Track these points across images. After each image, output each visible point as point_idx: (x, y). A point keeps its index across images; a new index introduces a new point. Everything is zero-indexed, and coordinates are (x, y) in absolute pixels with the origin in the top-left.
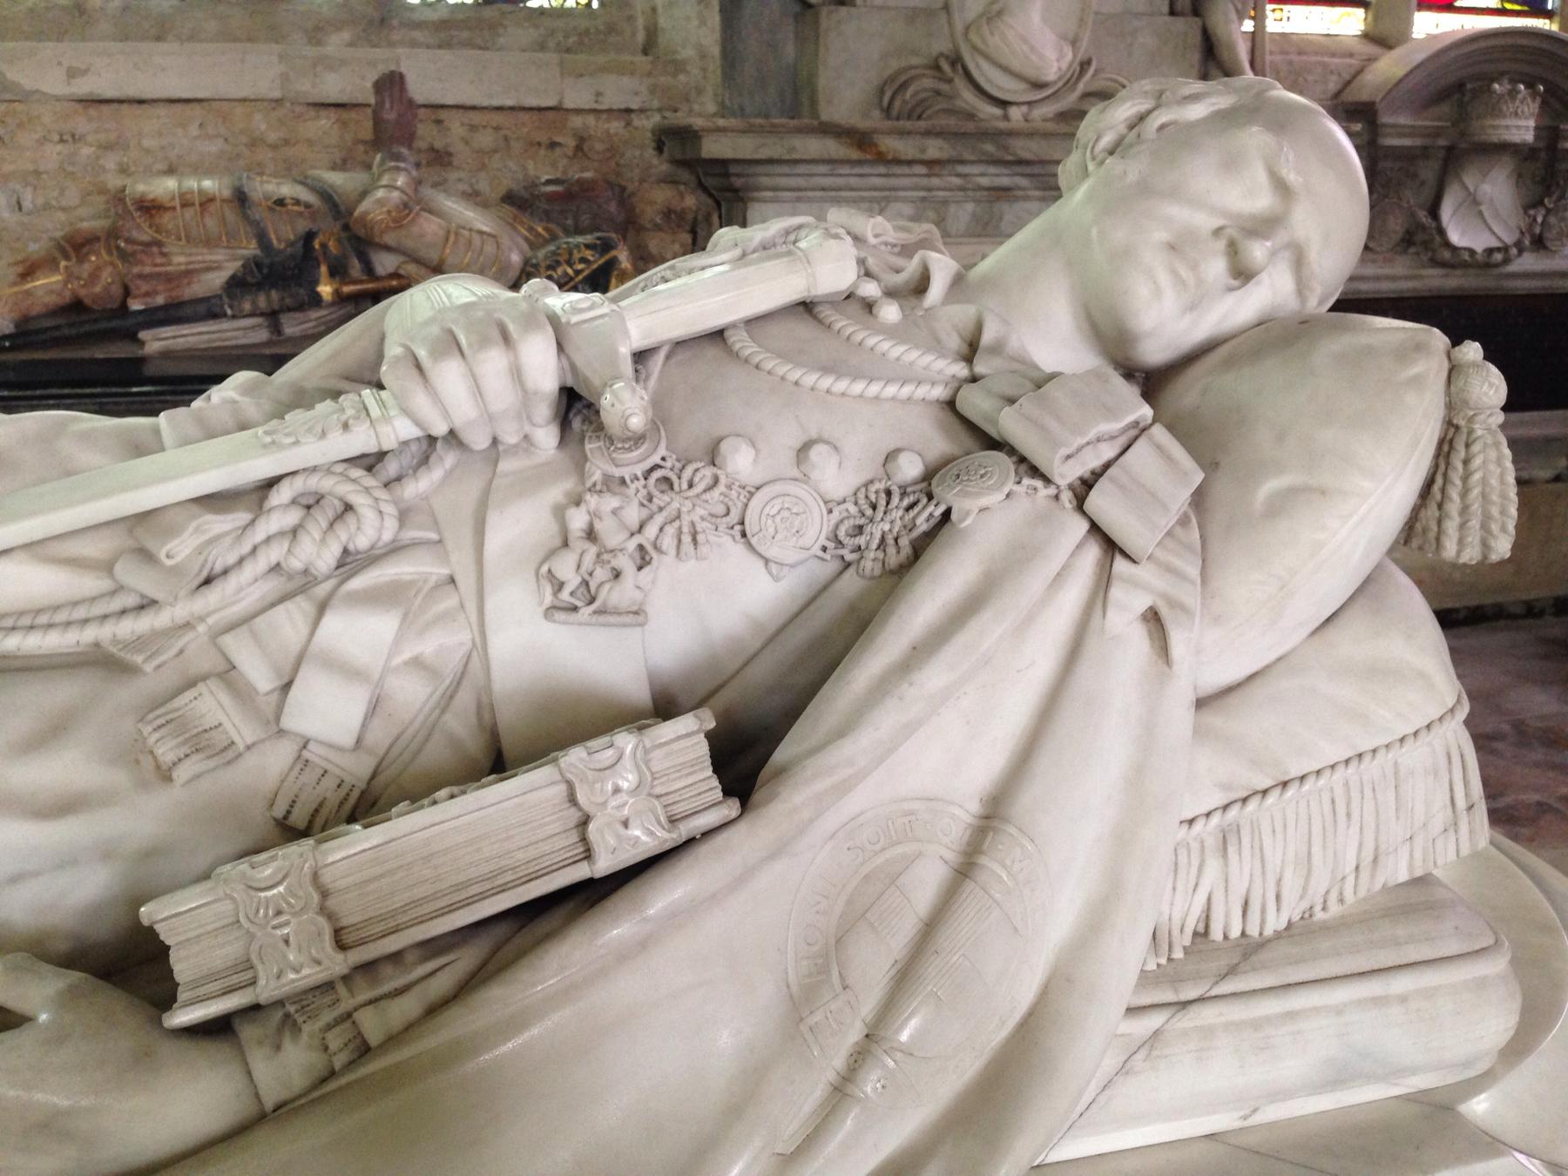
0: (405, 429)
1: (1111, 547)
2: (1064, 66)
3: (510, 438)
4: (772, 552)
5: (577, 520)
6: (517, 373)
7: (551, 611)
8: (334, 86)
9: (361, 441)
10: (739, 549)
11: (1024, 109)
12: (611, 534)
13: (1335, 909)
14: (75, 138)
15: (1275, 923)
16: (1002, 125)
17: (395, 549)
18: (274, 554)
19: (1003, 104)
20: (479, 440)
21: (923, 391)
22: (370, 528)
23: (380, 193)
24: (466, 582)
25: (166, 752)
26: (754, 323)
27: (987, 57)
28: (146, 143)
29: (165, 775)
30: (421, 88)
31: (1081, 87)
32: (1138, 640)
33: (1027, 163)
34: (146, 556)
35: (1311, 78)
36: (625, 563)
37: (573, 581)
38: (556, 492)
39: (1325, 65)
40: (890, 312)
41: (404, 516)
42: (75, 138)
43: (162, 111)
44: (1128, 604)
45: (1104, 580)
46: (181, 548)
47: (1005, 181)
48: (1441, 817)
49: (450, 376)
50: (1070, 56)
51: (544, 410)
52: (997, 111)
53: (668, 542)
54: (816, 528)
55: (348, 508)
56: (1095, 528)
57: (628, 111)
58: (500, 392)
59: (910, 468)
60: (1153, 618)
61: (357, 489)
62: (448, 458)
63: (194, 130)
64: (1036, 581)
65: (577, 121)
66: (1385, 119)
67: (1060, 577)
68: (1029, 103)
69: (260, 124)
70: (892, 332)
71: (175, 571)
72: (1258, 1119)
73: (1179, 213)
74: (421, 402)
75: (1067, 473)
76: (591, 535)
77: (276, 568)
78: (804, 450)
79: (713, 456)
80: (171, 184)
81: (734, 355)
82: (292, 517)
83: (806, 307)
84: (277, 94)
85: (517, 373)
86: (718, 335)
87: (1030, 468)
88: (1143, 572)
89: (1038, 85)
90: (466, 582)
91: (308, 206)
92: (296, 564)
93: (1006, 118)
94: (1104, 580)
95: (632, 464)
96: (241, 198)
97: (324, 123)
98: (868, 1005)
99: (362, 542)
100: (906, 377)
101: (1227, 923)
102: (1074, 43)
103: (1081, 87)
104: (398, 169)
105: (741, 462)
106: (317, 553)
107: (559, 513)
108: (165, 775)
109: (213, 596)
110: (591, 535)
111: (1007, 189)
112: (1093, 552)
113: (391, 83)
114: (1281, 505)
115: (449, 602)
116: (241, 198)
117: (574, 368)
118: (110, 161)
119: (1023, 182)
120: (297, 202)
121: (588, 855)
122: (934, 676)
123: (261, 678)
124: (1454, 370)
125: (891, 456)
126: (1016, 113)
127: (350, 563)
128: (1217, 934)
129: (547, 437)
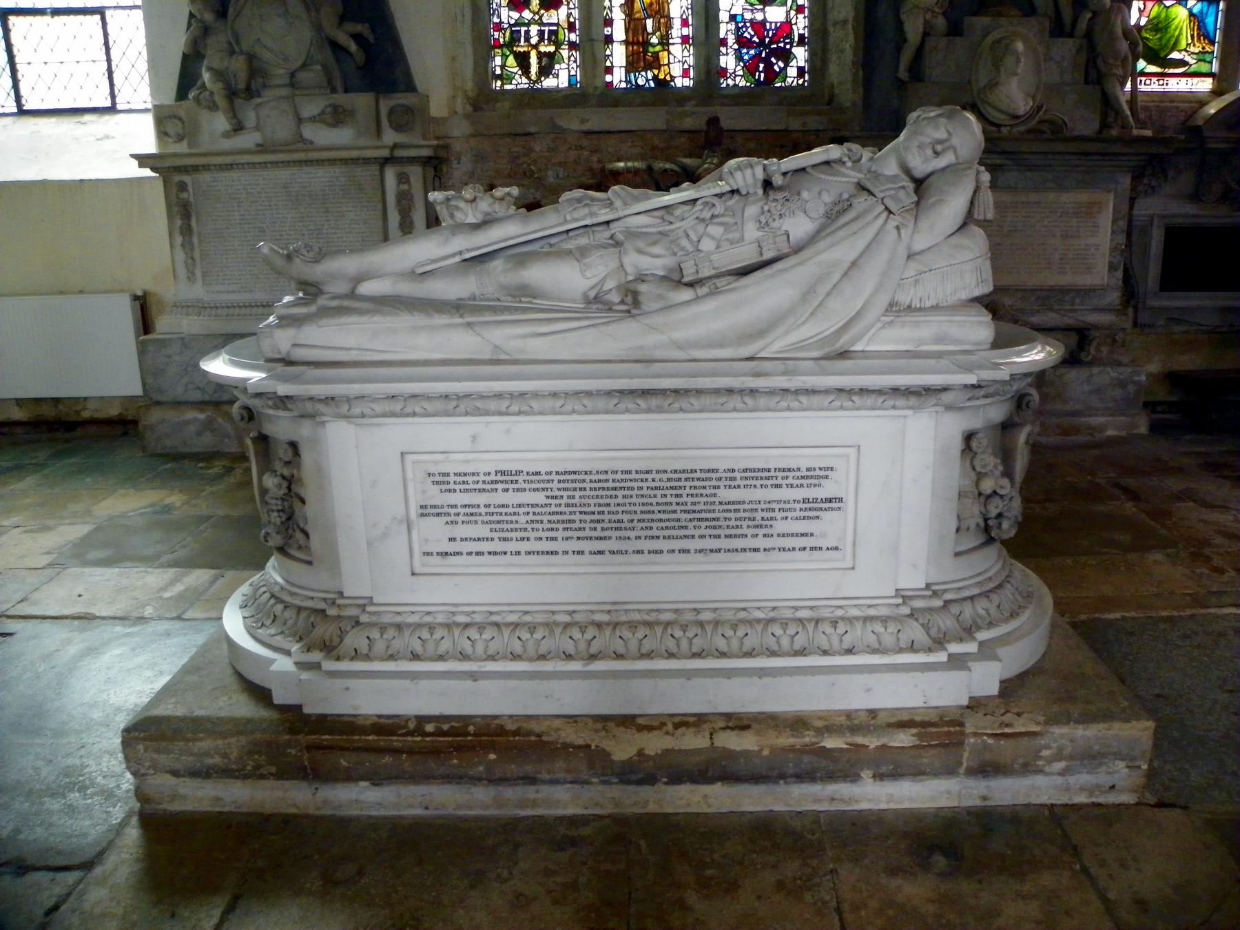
0: (728, 188)
1: (890, 212)
2: (1028, 108)
3: (751, 191)
4: (811, 215)
5: (766, 208)
6: (754, 175)
7: (758, 229)
8: (688, 123)
9: (717, 191)
10: (803, 215)
11: (1008, 128)
12: (773, 210)
13: (945, 304)
14: (581, 148)
15: (928, 304)
16: (996, 135)
17: (723, 215)
18: (698, 214)
19: (999, 126)
20: (744, 192)
21: (852, 180)
22: (719, 209)
23: (706, 166)
24: (740, 224)
25: (676, 250)
26: (814, 166)
27: (990, 105)
28: (610, 149)
29: (675, 254)
30: (725, 123)
31: (1037, 118)
32: (895, 232)
33: (1011, 153)
34: (672, 214)
35: (1169, 114)
36: (776, 217)
37: (764, 221)
38: (762, 203)
39: (1177, 108)
40: (849, 164)
41: (726, 210)
42: (581, 148)
43: (617, 136)
44: (892, 223)
45: (888, 218)
46: (678, 212)
47: (998, 161)
48: (974, 283)
49: (738, 175)
50: (1031, 104)
51: (759, 185)
52: (995, 129)
53: (787, 214)
54: (822, 211)
55: (714, 205)
56: (887, 208)
57: (818, 131)
58: (750, 180)
59: (845, 196)
60: (898, 228)
61: (716, 201)
62: (736, 197)
63: (629, 144)
64: (870, 217)
65: (795, 135)
66: (1207, 134)
67: (877, 217)
68: (1011, 125)
69: (656, 141)
70: (848, 168)
71: (677, 217)
72: (919, 349)
73: (921, 138)
74: (731, 181)
75: (880, 195)
76: (769, 211)
77: (697, 218)
78: (820, 193)
79: (799, 194)
80: (622, 164)
81: (807, 173)
82: (701, 207)
83: (827, 163)
84: (664, 127)
85: (754, 175)
86: (803, 170)
87: (871, 193)
88: (896, 217)
89: (1016, 117)
90: (740, 224)
91: (676, 172)
92: (702, 216)
93: (999, 132)
94: (888, 218)
95: (779, 196)
96: (650, 169)
97: (683, 140)
98: (820, 299)
99: (716, 213)
100: (850, 177)
101: (916, 303)
102: (1034, 98)
103: (1037, 118)
104: (714, 156)
105: (805, 195)
106: (707, 214)
107: (762, 208)
108: (675, 254)
109: (684, 222)
110: (769, 211)
111: (1001, 166)
112: (886, 213)
113: (714, 121)
114: (933, 205)
115: (736, 227)
116: (650, 169)
117: (767, 175)
118: (595, 158)
119: (1008, 162)
120: (672, 170)
121: (761, 254)
122: (841, 233)
123: (695, 238)
124: (978, 172)
125: (841, 195)
126: (1004, 130)
127: (713, 216)
128: (913, 306)
129: (760, 192)
